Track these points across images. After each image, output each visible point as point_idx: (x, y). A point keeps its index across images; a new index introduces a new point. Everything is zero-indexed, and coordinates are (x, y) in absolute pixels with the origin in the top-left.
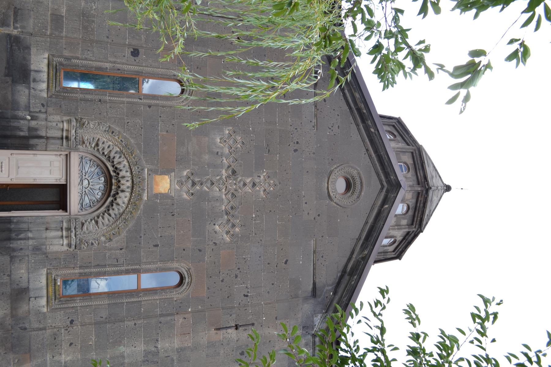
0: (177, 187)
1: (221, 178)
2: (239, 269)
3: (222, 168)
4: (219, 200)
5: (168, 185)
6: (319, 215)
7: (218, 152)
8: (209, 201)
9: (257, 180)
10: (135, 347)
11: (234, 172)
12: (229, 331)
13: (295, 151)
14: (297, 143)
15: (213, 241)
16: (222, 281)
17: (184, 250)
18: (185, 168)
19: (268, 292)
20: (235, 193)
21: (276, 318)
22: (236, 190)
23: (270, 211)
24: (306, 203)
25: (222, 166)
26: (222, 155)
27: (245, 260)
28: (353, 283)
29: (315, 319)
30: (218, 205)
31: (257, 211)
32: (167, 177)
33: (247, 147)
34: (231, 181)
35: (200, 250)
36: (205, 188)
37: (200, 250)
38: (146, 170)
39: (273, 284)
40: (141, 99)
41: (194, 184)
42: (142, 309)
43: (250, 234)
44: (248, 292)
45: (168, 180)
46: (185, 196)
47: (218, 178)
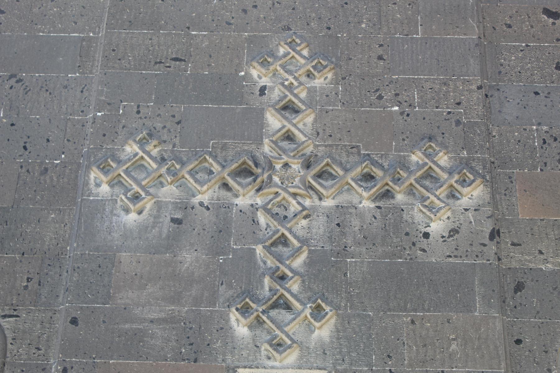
0: (292, 357)
3: (229, 207)
4: (340, 217)
7: (173, 220)
8: (344, 252)
9: (276, 94)
11: (244, 172)
15: (487, 241)
17: (518, 342)
18: (225, 330)
20: (316, 169)
22: (308, 165)
23: (380, 58)
25: (221, 209)
26: (185, 207)
27: (550, 141)
30: (356, 223)
31: (380, 97)
33: (159, 125)
34: (276, 179)
35: (519, 287)
37: (519, 287)
41: (282, 304)
43: (458, 123)
46: (324, 331)
47: (262, 219)
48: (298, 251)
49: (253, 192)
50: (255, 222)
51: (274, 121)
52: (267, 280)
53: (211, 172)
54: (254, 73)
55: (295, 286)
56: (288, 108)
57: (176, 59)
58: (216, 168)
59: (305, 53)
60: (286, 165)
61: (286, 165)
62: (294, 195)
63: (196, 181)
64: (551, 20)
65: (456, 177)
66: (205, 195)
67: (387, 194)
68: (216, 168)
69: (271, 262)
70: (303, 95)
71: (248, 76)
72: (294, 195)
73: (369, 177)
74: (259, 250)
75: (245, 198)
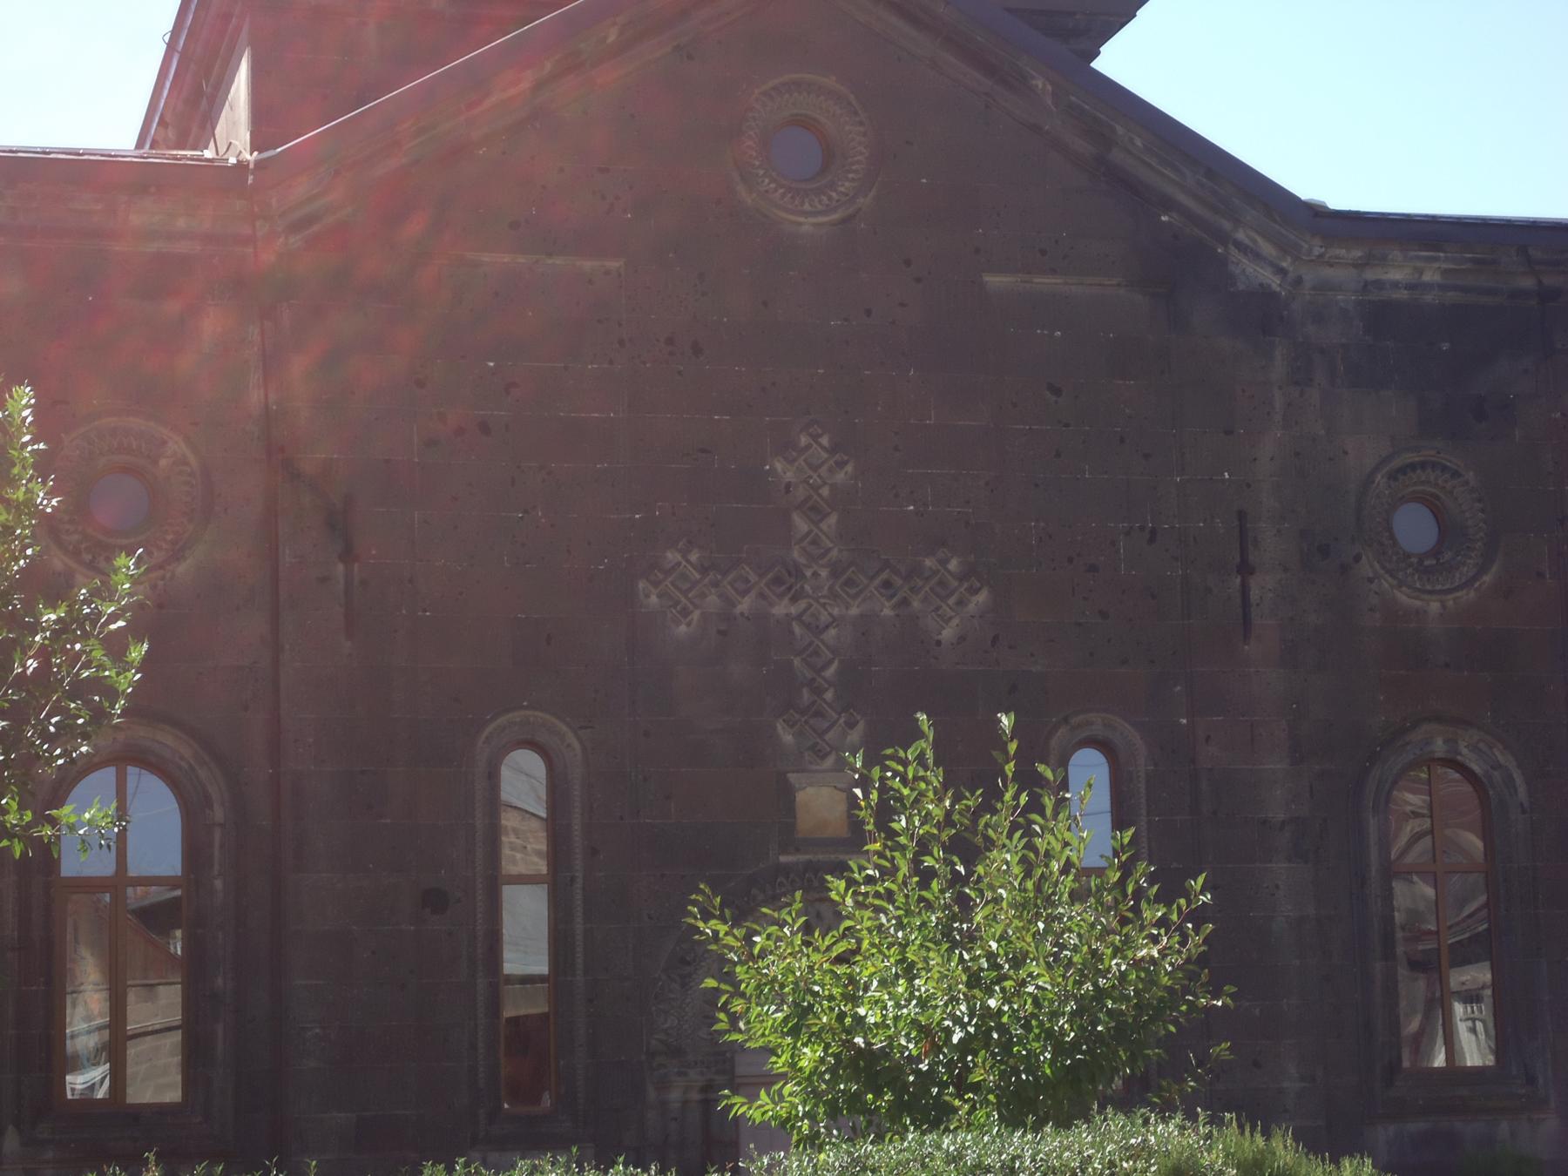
1: (799, 617)
2: (1070, 560)
5: (825, 791)
6: (908, 263)
7: (719, 632)
9: (801, 493)
10: (1277, 887)
11: (778, 581)
12: (1254, 594)
13: (697, 349)
14: (670, 341)
16: (1104, 614)
19: (1146, 456)
21: (1229, 432)
22: (835, 574)
23: (896, 449)
24: (868, 312)
28: (1139, 142)
29: (1241, 287)
31: (896, 496)
32: (800, 797)
34: (807, 587)
36: (830, 672)
38: (783, 859)
39: (1122, 440)
40: (573, 879)
41: (819, 714)
42: (1175, 865)
44: (1142, 528)
45: (810, 790)
47: (797, 629)
48: (830, 662)
49: (786, 601)
50: (792, 632)
51: (801, 524)
52: (805, 692)
53: (748, 581)
54: (779, 466)
55: (829, 695)
56: (815, 512)
57: (703, 451)
58: (753, 577)
59: (825, 441)
60: (815, 574)
61: (815, 574)
62: (824, 605)
63: (736, 590)
64: (1054, 398)
65: (966, 585)
66: (745, 605)
67: (905, 602)
68: (753, 577)
69: (809, 674)
70: (825, 492)
71: (773, 470)
72: (824, 605)
73: (887, 584)
74: (797, 662)
75: (781, 609)
